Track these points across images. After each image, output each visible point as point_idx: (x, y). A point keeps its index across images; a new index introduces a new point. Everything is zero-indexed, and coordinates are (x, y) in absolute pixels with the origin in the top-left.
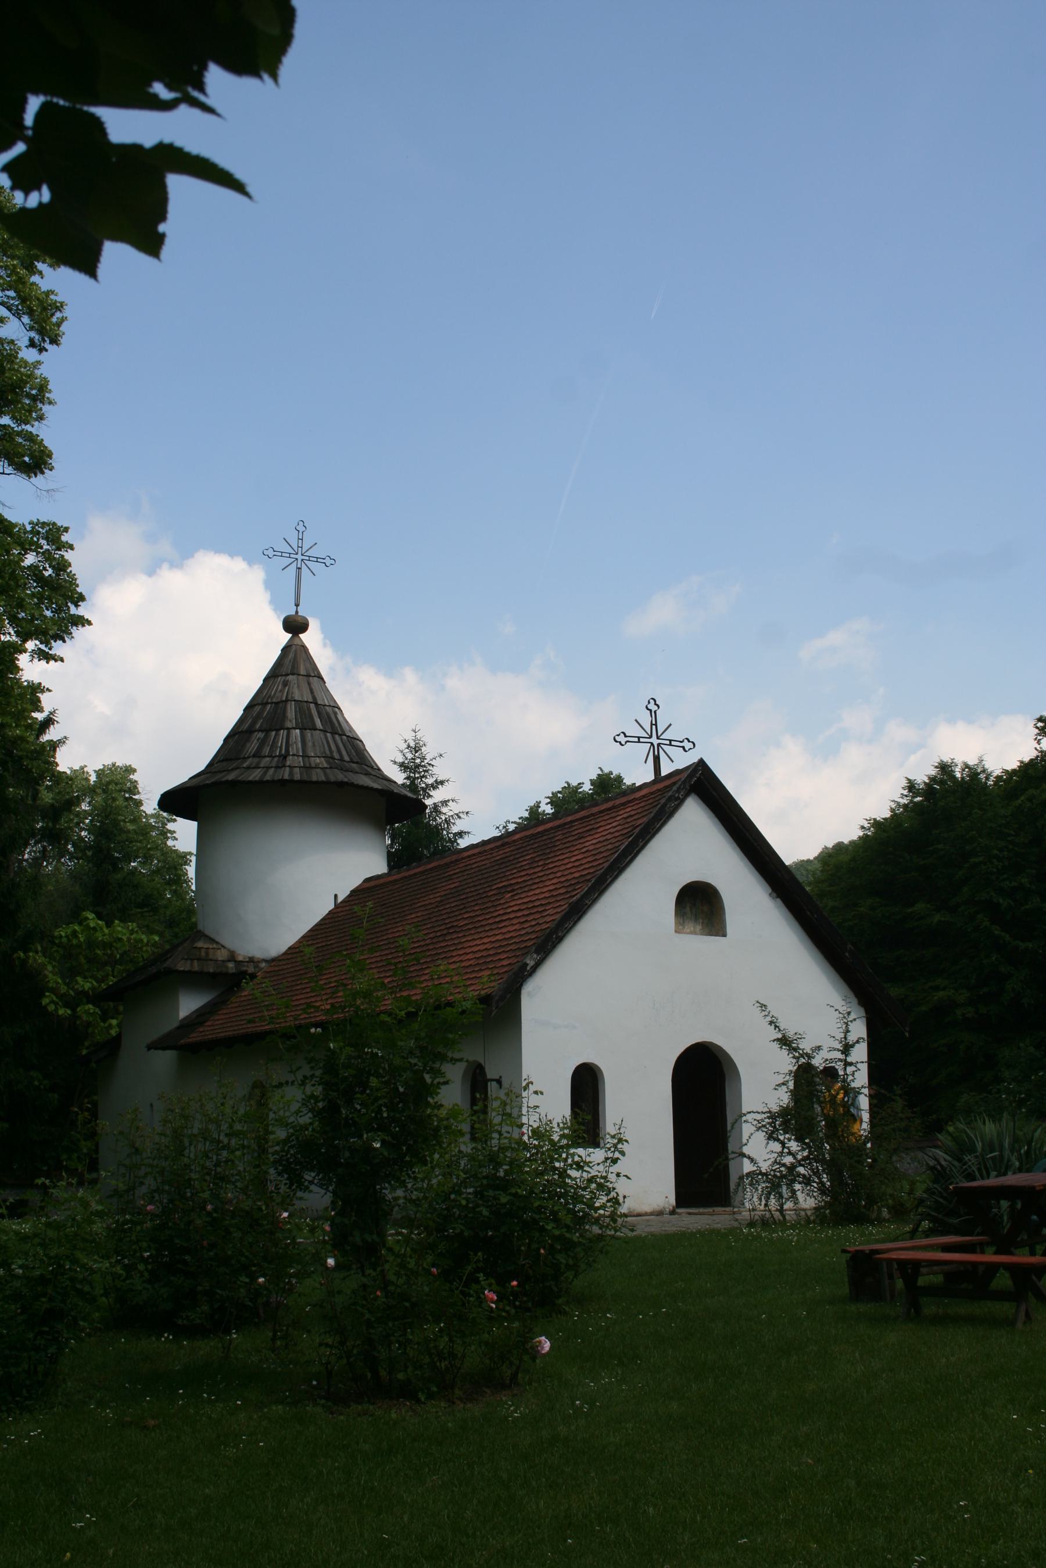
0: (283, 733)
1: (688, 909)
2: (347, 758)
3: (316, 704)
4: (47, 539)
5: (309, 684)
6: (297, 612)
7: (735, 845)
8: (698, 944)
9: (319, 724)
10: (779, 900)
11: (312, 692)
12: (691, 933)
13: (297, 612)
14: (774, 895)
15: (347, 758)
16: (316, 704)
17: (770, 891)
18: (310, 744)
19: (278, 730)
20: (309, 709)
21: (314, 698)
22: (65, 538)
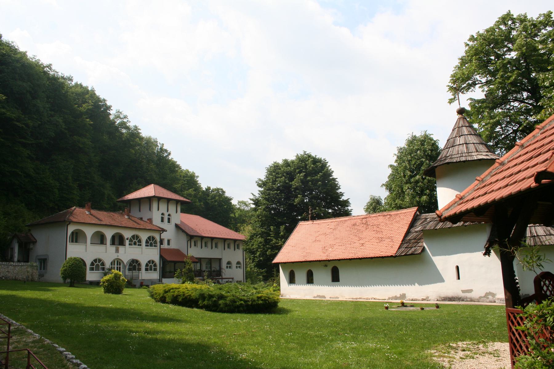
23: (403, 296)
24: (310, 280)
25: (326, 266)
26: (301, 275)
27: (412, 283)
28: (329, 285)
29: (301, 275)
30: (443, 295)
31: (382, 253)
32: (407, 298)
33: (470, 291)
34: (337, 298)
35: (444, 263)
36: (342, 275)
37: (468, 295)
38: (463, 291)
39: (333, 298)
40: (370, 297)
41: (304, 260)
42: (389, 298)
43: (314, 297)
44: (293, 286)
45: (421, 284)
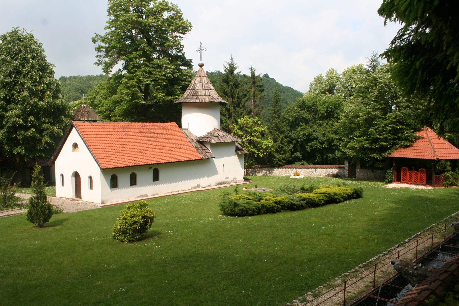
23: (199, 186)
24: (133, 182)
25: (150, 168)
26: (124, 179)
27: (202, 176)
28: (150, 185)
29: (124, 179)
30: (217, 182)
31: (193, 157)
32: (201, 186)
33: (228, 178)
34: (157, 194)
35: (218, 162)
36: (161, 175)
37: (227, 180)
38: (226, 178)
39: (154, 195)
40: (180, 190)
41: (137, 164)
42: (192, 188)
43: (138, 197)
44: (116, 191)
45: (208, 177)
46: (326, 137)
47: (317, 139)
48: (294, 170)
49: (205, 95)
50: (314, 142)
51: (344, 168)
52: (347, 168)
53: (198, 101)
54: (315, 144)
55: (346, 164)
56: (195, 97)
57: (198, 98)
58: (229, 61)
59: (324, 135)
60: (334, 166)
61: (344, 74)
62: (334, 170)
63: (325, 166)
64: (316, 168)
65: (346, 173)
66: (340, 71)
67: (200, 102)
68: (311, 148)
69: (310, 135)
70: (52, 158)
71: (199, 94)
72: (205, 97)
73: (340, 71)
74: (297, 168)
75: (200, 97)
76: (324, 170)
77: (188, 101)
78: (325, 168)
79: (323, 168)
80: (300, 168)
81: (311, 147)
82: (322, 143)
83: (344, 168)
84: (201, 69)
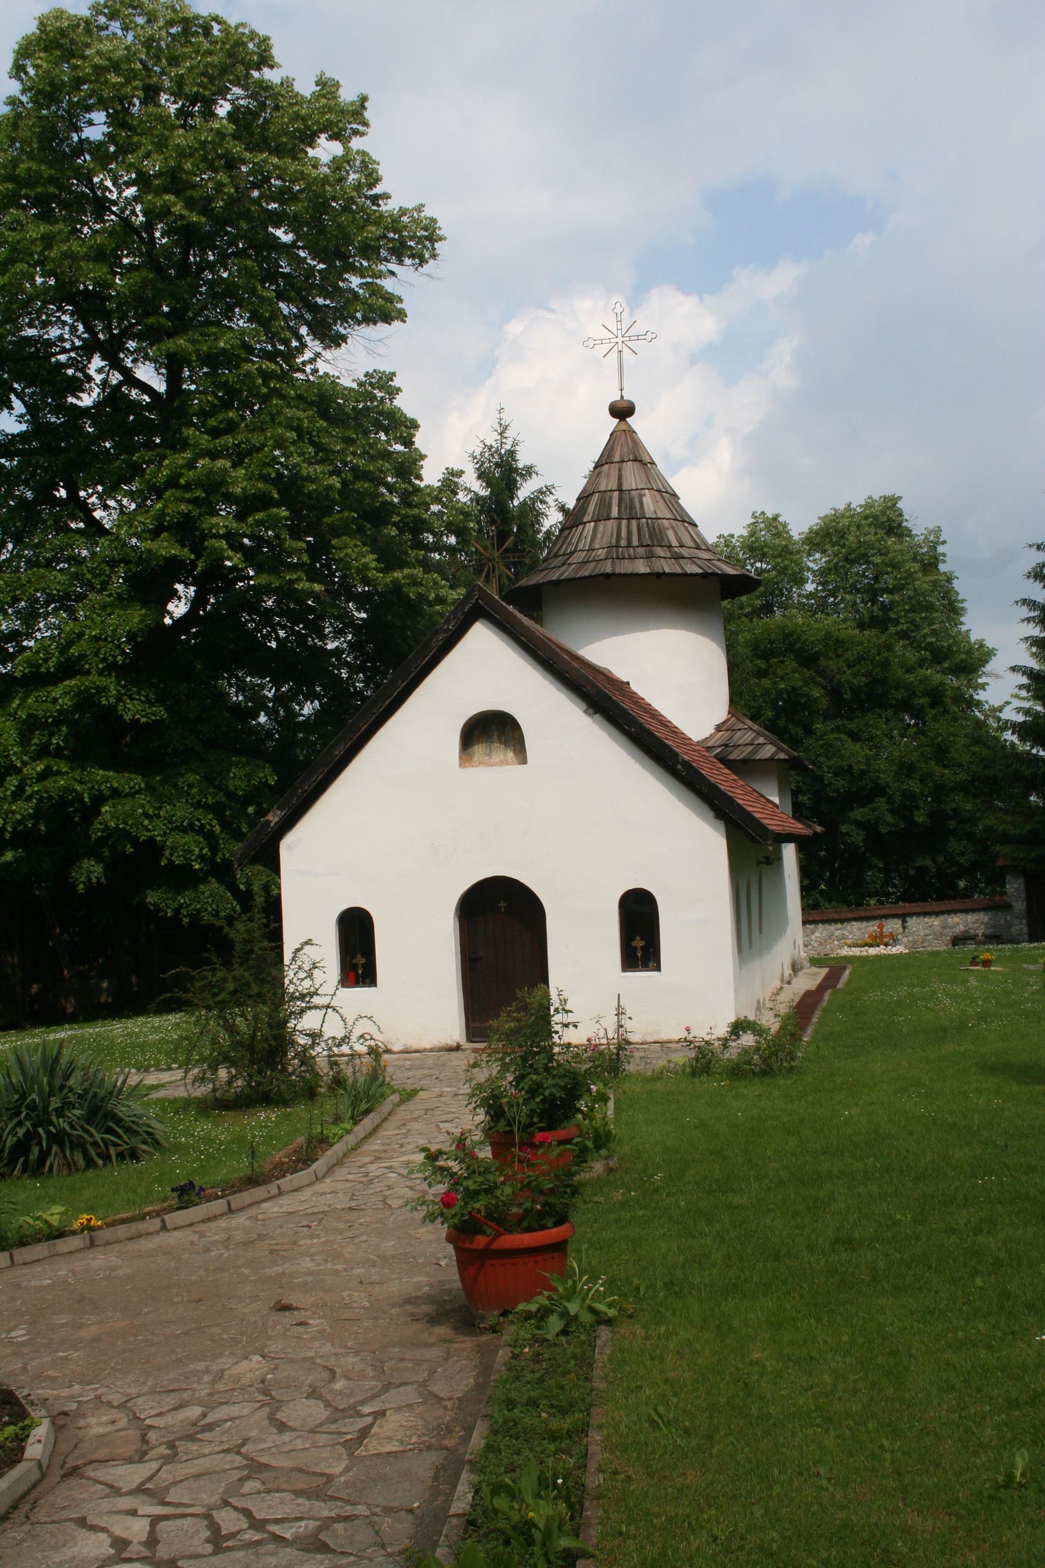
0: (581, 527)
1: (496, 738)
2: (635, 542)
3: (621, 490)
4: (378, 387)
5: (620, 470)
6: (622, 397)
7: (536, 664)
8: (495, 774)
9: (615, 512)
10: (598, 716)
11: (620, 478)
12: (502, 763)
13: (622, 397)
14: (591, 711)
15: (635, 542)
16: (621, 490)
17: (585, 707)
18: (599, 536)
19: (577, 526)
20: (611, 498)
21: (620, 485)
22: (396, 383)
46: (922, 781)
47: (879, 790)
48: (871, 927)
49: (698, 548)
50: (881, 802)
51: (1007, 907)
52: (1019, 905)
53: (700, 571)
54: (881, 812)
55: (1014, 888)
56: (659, 551)
57: (678, 557)
58: (492, 439)
59: (907, 769)
60: (968, 903)
61: (828, 534)
62: (970, 918)
63: (933, 906)
64: (903, 917)
65: (1020, 927)
66: (800, 524)
67: (705, 575)
68: (863, 833)
69: (863, 773)
70: (274, 818)
71: (674, 543)
72: (705, 555)
73: (800, 524)
74: (829, 921)
75: (684, 552)
76: (936, 922)
77: (641, 567)
78: (937, 914)
79: (930, 914)
80: (842, 921)
81: (867, 827)
82: (904, 809)
83: (1007, 907)
84: (623, 426)
